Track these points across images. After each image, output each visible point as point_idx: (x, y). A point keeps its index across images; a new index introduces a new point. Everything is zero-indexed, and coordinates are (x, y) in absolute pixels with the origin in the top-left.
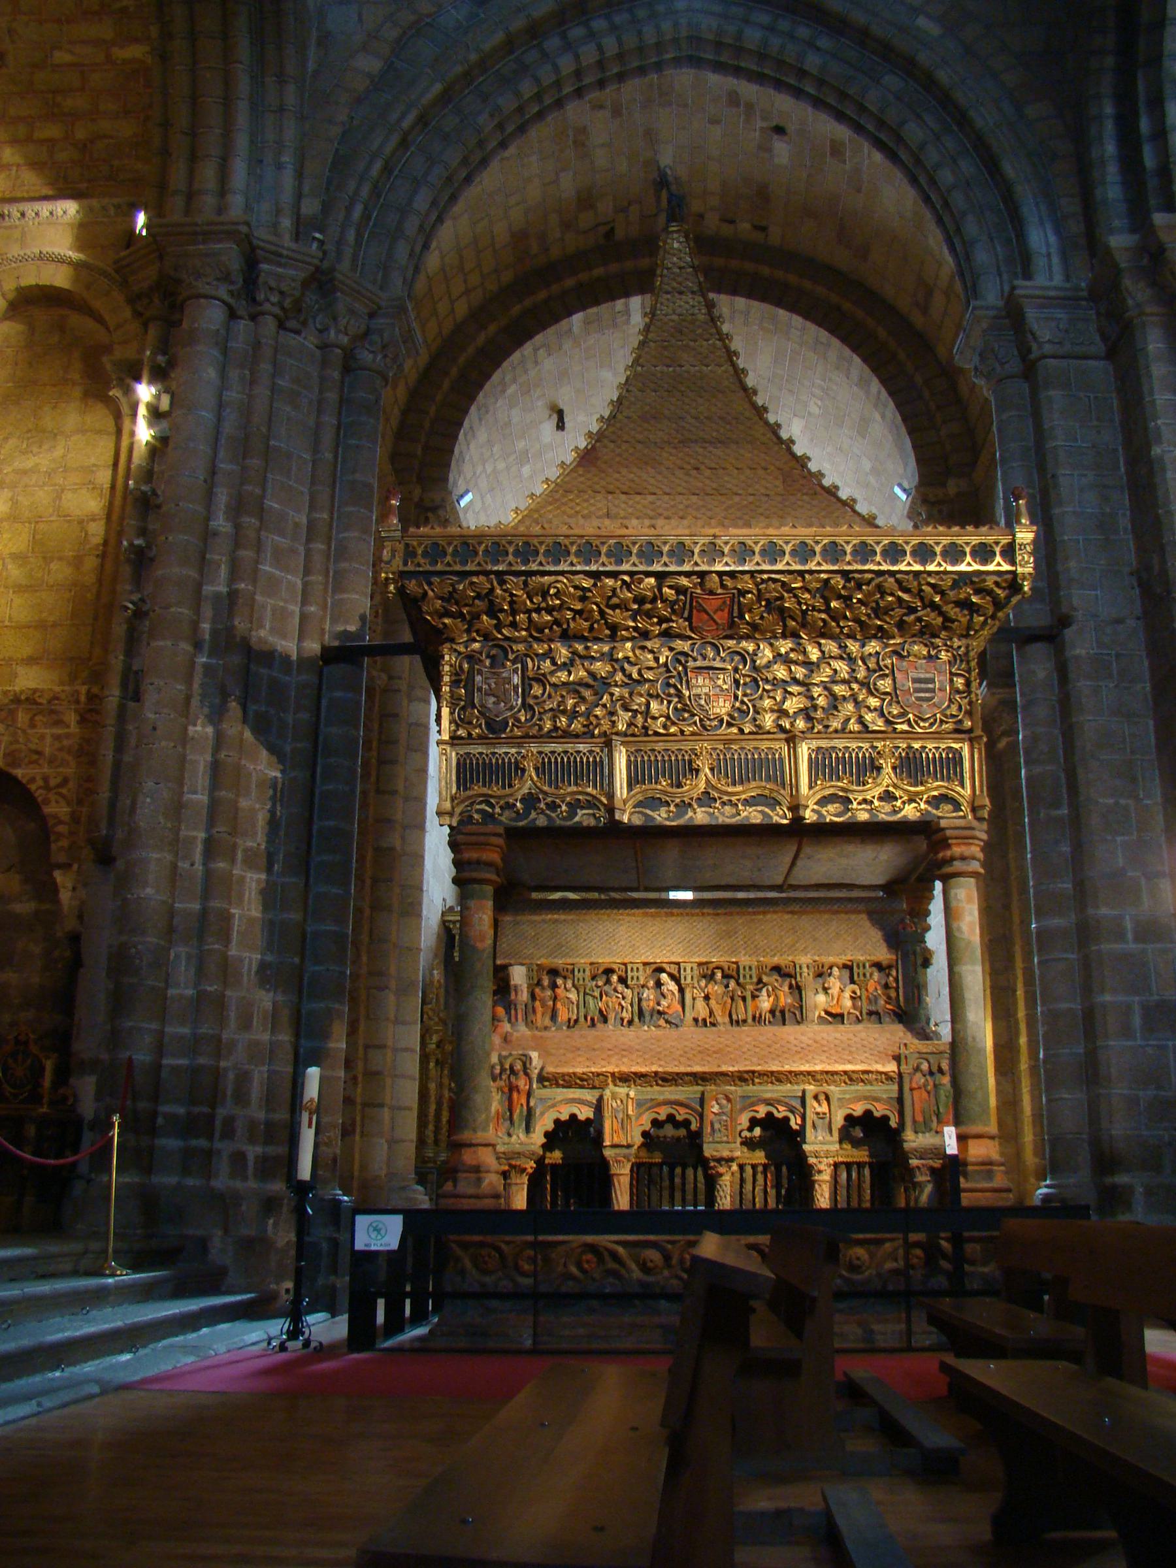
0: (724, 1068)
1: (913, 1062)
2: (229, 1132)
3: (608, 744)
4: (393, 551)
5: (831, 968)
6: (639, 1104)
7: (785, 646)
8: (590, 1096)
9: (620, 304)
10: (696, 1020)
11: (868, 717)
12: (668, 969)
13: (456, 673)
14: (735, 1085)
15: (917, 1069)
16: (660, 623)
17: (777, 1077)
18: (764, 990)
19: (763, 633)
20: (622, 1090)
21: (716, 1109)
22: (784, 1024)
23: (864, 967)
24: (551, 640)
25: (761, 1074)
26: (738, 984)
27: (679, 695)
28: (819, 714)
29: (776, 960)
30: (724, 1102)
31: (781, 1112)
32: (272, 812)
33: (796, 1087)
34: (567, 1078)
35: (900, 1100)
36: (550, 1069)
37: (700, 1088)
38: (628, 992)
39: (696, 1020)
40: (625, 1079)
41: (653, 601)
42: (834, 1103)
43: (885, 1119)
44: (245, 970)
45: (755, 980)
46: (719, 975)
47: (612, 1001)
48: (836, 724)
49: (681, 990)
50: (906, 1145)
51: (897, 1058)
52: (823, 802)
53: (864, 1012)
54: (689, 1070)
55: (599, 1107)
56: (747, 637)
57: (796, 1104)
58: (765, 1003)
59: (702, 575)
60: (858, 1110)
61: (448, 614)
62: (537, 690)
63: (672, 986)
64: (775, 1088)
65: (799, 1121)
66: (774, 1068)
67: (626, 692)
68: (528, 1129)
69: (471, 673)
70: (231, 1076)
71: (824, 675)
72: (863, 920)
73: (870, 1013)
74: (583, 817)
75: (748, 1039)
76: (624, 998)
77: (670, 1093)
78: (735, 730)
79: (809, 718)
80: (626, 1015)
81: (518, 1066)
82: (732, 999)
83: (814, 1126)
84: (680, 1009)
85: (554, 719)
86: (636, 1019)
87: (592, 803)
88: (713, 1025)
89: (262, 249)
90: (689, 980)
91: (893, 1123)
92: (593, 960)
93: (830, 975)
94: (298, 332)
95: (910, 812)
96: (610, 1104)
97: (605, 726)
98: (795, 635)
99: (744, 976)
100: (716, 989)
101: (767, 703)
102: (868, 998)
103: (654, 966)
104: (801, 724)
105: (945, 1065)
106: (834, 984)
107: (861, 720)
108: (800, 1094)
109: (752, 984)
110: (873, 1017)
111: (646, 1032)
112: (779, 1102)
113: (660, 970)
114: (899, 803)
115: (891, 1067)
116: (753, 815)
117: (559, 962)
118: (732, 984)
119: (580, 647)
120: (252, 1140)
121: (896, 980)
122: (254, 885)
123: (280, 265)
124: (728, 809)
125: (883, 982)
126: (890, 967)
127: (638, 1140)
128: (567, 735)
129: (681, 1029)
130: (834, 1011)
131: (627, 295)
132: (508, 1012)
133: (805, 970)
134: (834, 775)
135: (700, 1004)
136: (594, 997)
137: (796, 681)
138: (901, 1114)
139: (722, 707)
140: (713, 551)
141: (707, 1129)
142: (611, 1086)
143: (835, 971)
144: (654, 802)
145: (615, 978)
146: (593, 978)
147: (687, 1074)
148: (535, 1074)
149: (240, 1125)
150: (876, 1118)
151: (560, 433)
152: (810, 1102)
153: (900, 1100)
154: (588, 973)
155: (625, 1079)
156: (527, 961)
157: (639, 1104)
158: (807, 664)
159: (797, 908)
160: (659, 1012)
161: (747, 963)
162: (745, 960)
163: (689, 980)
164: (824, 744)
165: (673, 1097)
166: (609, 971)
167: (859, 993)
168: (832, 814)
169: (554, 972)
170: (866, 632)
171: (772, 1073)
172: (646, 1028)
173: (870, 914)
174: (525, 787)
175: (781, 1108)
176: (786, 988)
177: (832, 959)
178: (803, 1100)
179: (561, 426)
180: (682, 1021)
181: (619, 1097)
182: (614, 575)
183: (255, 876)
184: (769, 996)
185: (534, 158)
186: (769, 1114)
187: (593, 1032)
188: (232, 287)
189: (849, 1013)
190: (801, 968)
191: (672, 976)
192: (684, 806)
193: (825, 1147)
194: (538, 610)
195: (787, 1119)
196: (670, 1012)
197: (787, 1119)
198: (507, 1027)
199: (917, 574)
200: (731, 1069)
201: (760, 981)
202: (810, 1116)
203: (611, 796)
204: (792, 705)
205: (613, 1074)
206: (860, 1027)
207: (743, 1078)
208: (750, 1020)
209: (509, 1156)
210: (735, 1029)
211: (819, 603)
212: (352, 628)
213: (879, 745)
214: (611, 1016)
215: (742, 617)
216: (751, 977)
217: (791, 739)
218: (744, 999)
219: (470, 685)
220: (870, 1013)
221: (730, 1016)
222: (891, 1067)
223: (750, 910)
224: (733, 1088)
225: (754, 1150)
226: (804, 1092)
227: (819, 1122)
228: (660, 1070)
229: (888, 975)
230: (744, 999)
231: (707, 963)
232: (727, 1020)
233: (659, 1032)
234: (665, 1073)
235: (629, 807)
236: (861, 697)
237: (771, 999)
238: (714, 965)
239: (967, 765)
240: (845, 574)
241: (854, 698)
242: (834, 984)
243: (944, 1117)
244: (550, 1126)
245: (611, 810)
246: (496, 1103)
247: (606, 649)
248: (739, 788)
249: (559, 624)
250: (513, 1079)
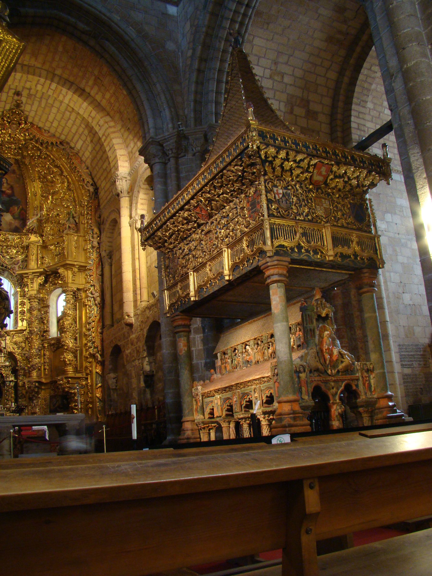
40: (217, 391)
44: (200, 366)
89: (161, 141)
94: (185, 156)
122: (199, 339)
123: (167, 142)
132: (215, 370)
171: (242, 383)
183: (199, 336)
185: (301, 17)
188: (159, 157)
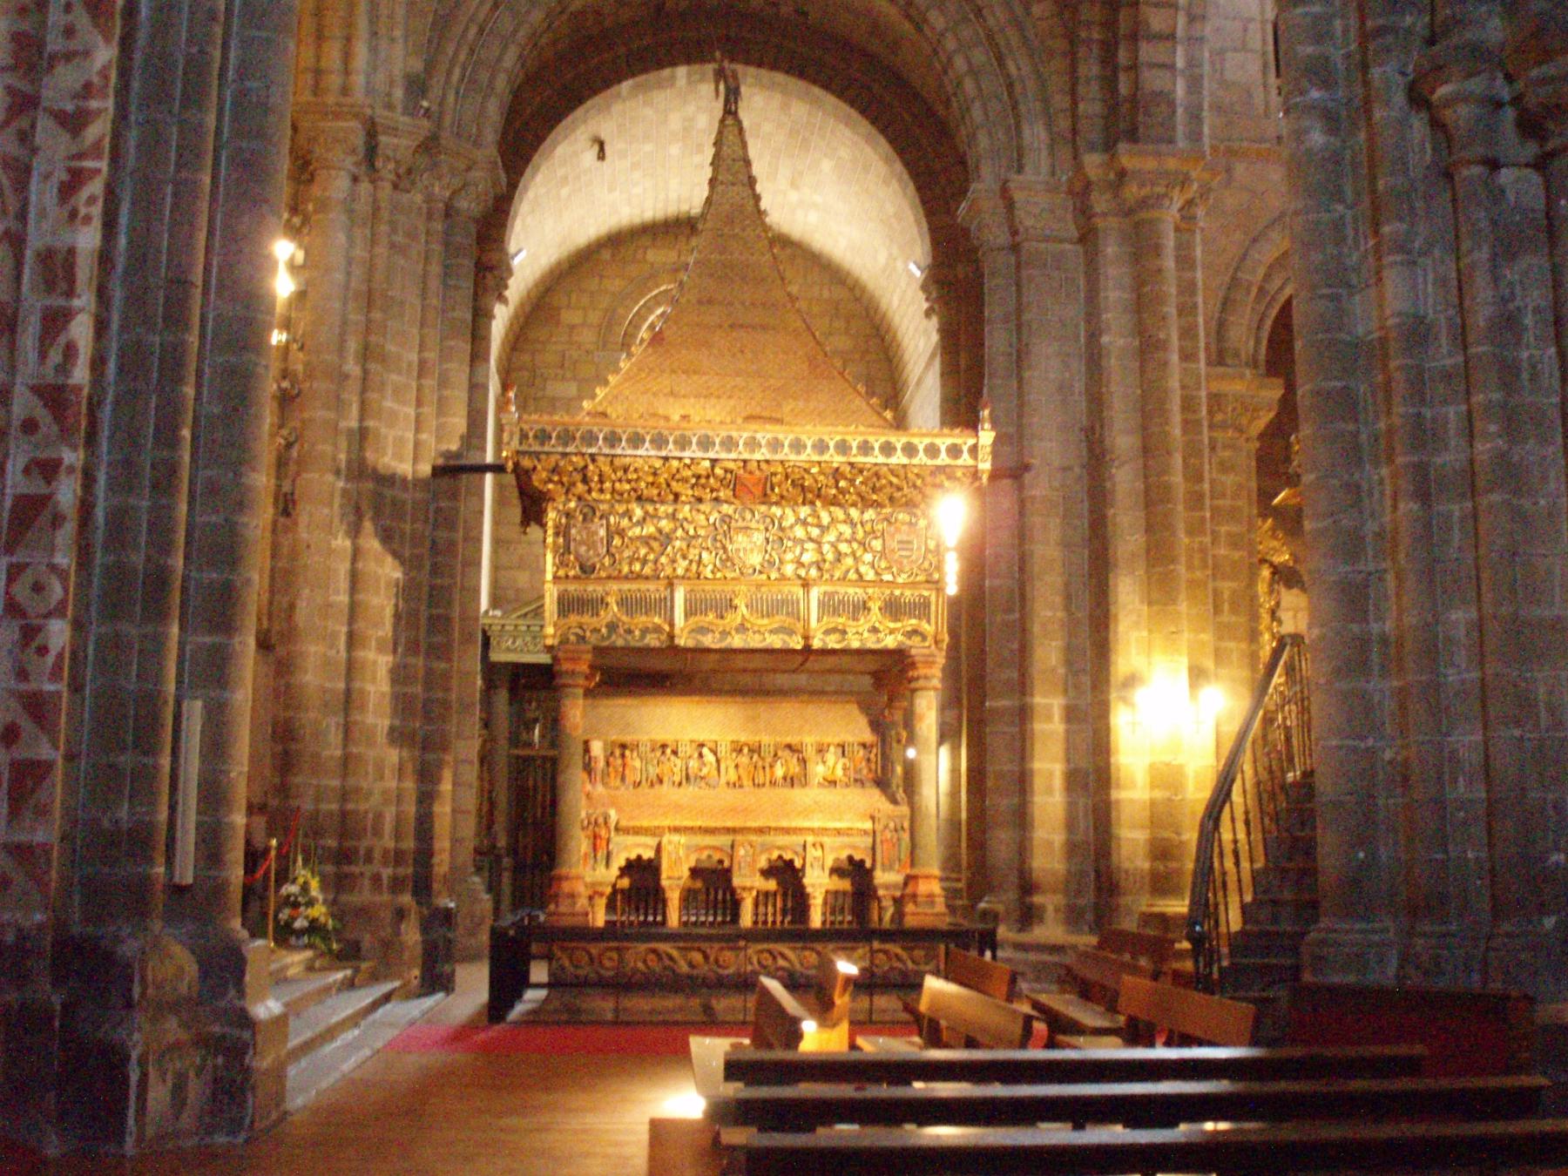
1: (883, 822)
2: (369, 859)
3: (671, 585)
4: (512, 434)
6: (688, 848)
7: (804, 511)
8: (653, 841)
9: (667, 72)
11: (863, 569)
13: (557, 527)
15: (886, 827)
16: (712, 491)
17: (787, 831)
19: (788, 501)
20: (676, 838)
24: (628, 502)
25: (776, 829)
27: (724, 548)
28: (827, 566)
29: (788, 740)
31: (788, 856)
32: (396, 605)
35: (873, 848)
36: (624, 823)
38: (678, 762)
40: (676, 830)
41: (708, 477)
43: (862, 862)
46: (746, 750)
47: (666, 767)
48: (837, 574)
49: (718, 761)
51: (873, 818)
52: (827, 632)
55: (658, 850)
56: (776, 503)
57: (800, 850)
58: (779, 772)
59: (745, 461)
60: (844, 855)
61: (550, 481)
62: (617, 541)
67: (684, 546)
68: (608, 865)
69: (568, 527)
70: (371, 816)
71: (831, 537)
72: (854, 709)
74: (652, 641)
78: (764, 577)
79: (819, 569)
80: (677, 779)
81: (601, 820)
85: (630, 564)
87: (658, 629)
88: (741, 786)
91: (868, 864)
95: (890, 642)
97: (669, 571)
98: (812, 503)
100: (744, 760)
101: (789, 556)
104: (814, 572)
105: (906, 825)
106: (831, 757)
107: (857, 571)
111: (690, 790)
113: (702, 745)
114: (881, 635)
115: (868, 825)
116: (776, 642)
117: (627, 739)
118: (756, 757)
119: (650, 508)
120: (385, 864)
124: (758, 637)
127: (686, 873)
128: (639, 577)
131: (673, 64)
134: (836, 612)
135: (732, 771)
137: (811, 540)
138: (874, 861)
139: (755, 559)
140: (753, 444)
141: (735, 867)
143: (832, 749)
144: (703, 630)
145: (668, 751)
149: (377, 854)
151: (599, 164)
152: (809, 848)
153: (873, 848)
155: (676, 830)
157: (688, 848)
158: (819, 526)
160: (702, 778)
162: (766, 739)
164: (830, 588)
166: (664, 746)
168: (833, 643)
169: (623, 746)
170: (866, 503)
173: (859, 703)
174: (605, 617)
177: (829, 740)
178: (805, 847)
179: (601, 155)
181: (672, 842)
182: (680, 459)
187: (652, 791)
192: (725, 634)
194: (620, 480)
198: (589, 787)
199: (904, 466)
203: (672, 625)
204: (806, 558)
207: (761, 831)
209: (593, 884)
211: (831, 482)
212: (454, 447)
213: (870, 591)
214: (665, 779)
215: (772, 489)
217: (806, 584)
219: (567, 536)
222: (868, 825)
233: (702, 792)
235: (685, 634)
236: (858, 554)
239: (933, 608)
240: (852, 465)
241: (853, 554)
242: (831, 757)
244: (623, 863)
245: (671, 637)
246: (584, 846)
247: (670, 510)
248: (765, 621)
249: (635, 490)
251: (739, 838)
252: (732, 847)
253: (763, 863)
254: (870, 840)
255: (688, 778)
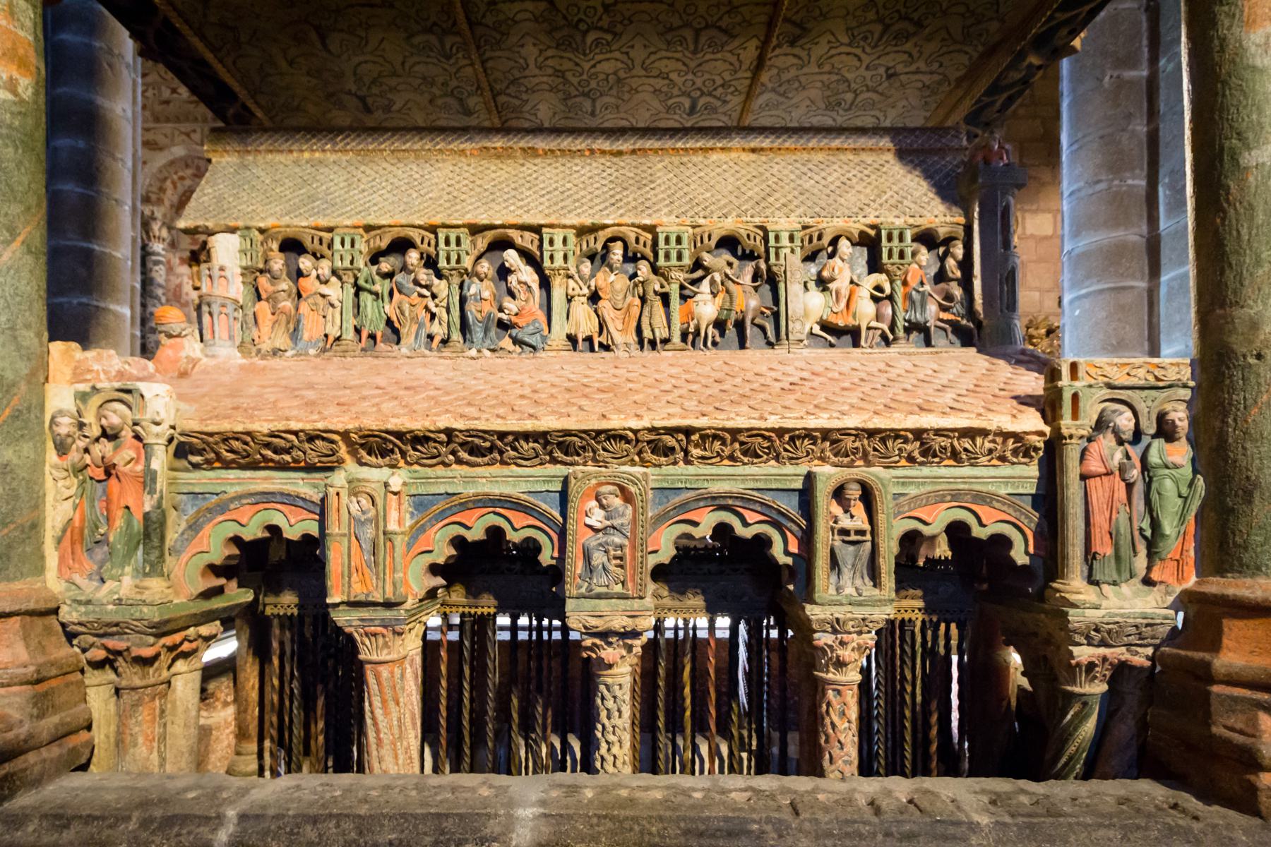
0: (615, 422)
5: (834, 242)
10: (572, 339)
12: (518, 241)
14: (644, 463)
18: (706, 282)
20: (375, 474)
21: (597, 518)
22: (742, 346)
23: (901, 239)
26: (655, 270)
30: (617, 502)
33: (789, 469)
34: (236, 445)
36: (195, 426)
37: (560, 470)
38: (441, 286)
39: (572, 339)
42: (885, 506)
43: (1001, 542)
45: (687, 261)
46: (617, 251)
49: (545, 284)
50: (1074, 616)
53: (900, 324)
54: (529, 425)
57: (790, 505)
58: (706, 308)
63: (527, 274)
64: (740, 470)
65: (794, 548)
66: (741, 423)
73: (912, 327)
75: (674, 371)
76: (434, 296)
77: (493, 479)
80: (438, 330)
82: (643, 299)
83: (834, 563)
84: (542, 318)
86: (456, 336)
88: (606, 348)
90: (559, 261)
91: (1020, 556)
92: (371, 220)
93: (831, 256)
96: (345, 509)
99: (667, 257)
102: (908, 297)
103: (490, 235)
108: (798, 484)
109: (681, 268)
110: (914, 335)
112: (746, 500)
118: (644, 269)
121: (966, 265)
125: (933, 270)
126: (948, 241)
129: (541, 354)
130: (841, 323)
133: (785, 241)
135: (582, 309)
136: (376, 294)
141: (575, 566)
142: (350, 465)
146: (374, 259)
147: (527, 436)
148: (157, 436)
150: (978, 541)
152: (826, 507)
154: (361, 245)
156: (240, 223)
159: (766, 143)
160: (503, 325)
161: (674, 230)
162: (668, 224)
163: (559, 261)
165: (496, 490)
166: (401, 246)
167: (888, 290)
169: (292, 246)
172: (473, 352)
175: (751, 517)
176: (747, 279)
177: (839, 224)
178: (806, 495)
180: (544, 339)
184: (714, 295)
186: (722, 530)
189: (869, 328)
190: (777, 238)
191: (526, 255)
193: (859, 612)
195: (762, 542)
196: (521, 322)
197: (762, 542)
198: (191, 347)
200: (635, 424)
201: (698, 264)
202: (824, 539)
205: (345, 435)
206: (894, 349)
208: (676, 339)
210: (648, 353)
214: (408, 331)
216: (680, 257)
218: (665, 299)
220: (912, 327)
221: (639, 331)
223: (679, 145)
224: (638, 470)
225: (683, 593)
226: (810, 478)
227: (846, 553)
228: (459, 425)
229: (942, 259)
230: (665, 299)
231: (594, 229)
232: (632, 338)
234: (469, 432)
237: (719, 300)
238: (608, 233)
243: (1171, 547)
250: (106, 447)
251: (583, 471)
252: (564, 496)
253: (664, 547)
254: (1033, 470)
255: (465, 327)
